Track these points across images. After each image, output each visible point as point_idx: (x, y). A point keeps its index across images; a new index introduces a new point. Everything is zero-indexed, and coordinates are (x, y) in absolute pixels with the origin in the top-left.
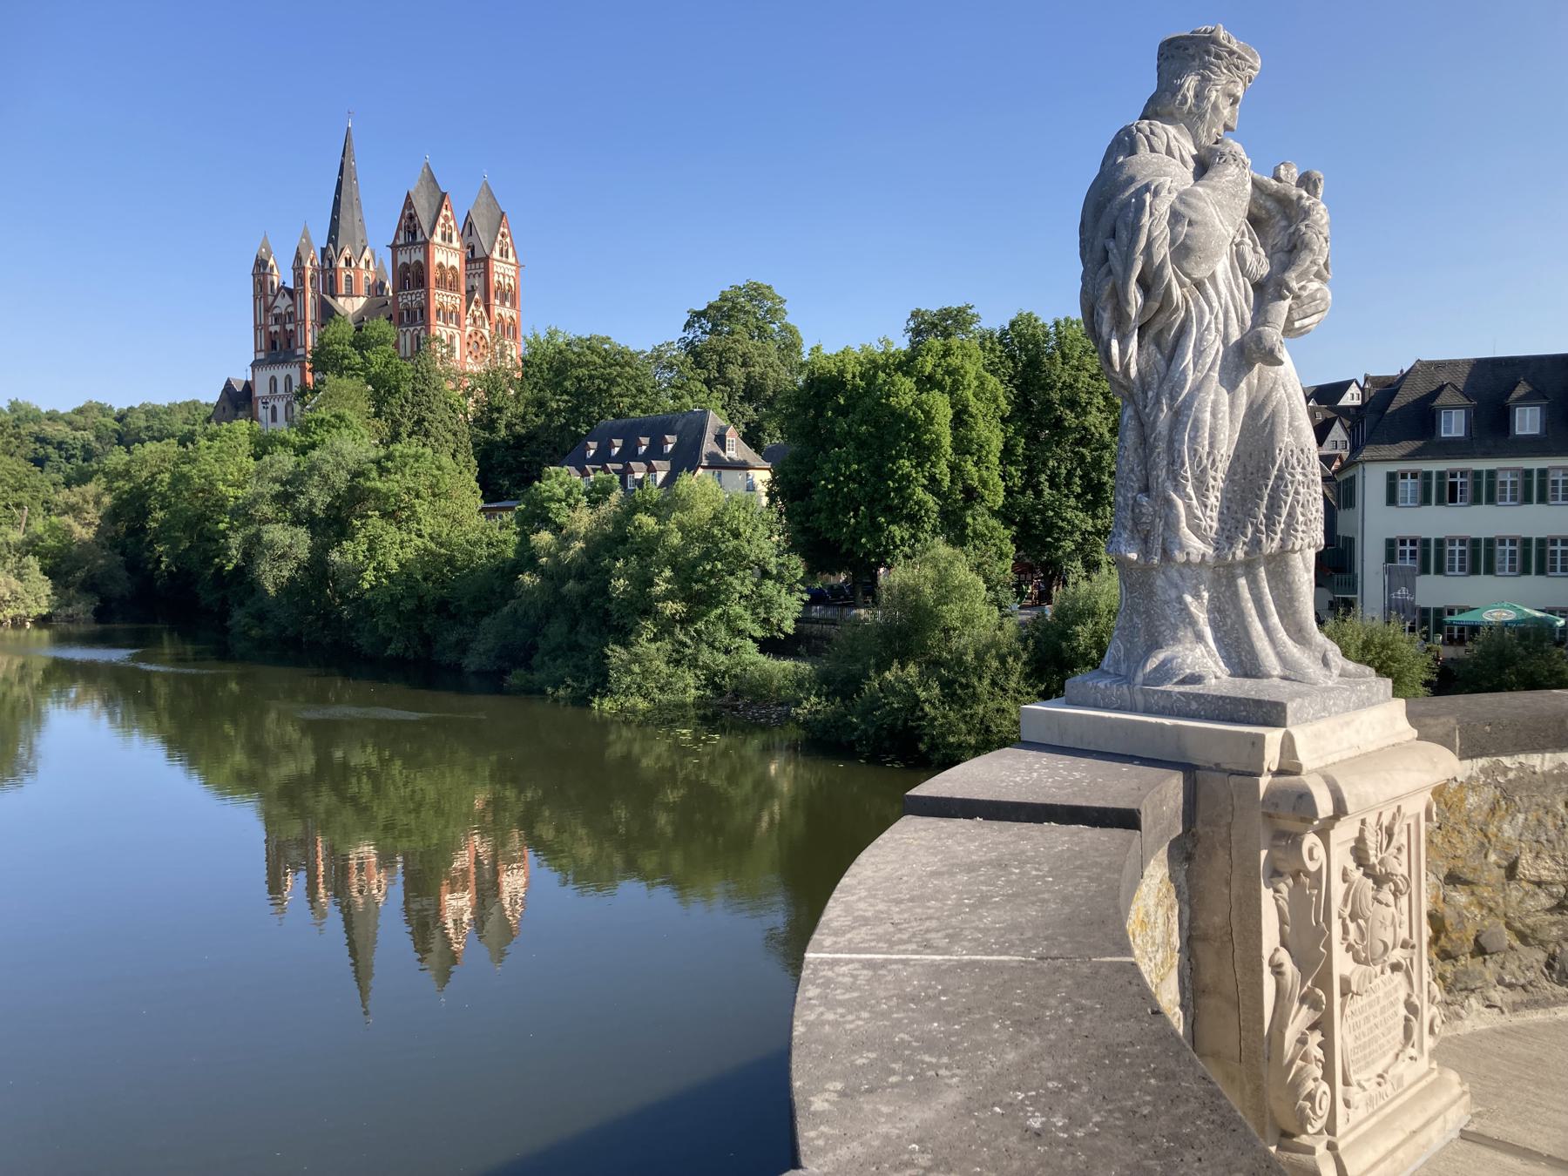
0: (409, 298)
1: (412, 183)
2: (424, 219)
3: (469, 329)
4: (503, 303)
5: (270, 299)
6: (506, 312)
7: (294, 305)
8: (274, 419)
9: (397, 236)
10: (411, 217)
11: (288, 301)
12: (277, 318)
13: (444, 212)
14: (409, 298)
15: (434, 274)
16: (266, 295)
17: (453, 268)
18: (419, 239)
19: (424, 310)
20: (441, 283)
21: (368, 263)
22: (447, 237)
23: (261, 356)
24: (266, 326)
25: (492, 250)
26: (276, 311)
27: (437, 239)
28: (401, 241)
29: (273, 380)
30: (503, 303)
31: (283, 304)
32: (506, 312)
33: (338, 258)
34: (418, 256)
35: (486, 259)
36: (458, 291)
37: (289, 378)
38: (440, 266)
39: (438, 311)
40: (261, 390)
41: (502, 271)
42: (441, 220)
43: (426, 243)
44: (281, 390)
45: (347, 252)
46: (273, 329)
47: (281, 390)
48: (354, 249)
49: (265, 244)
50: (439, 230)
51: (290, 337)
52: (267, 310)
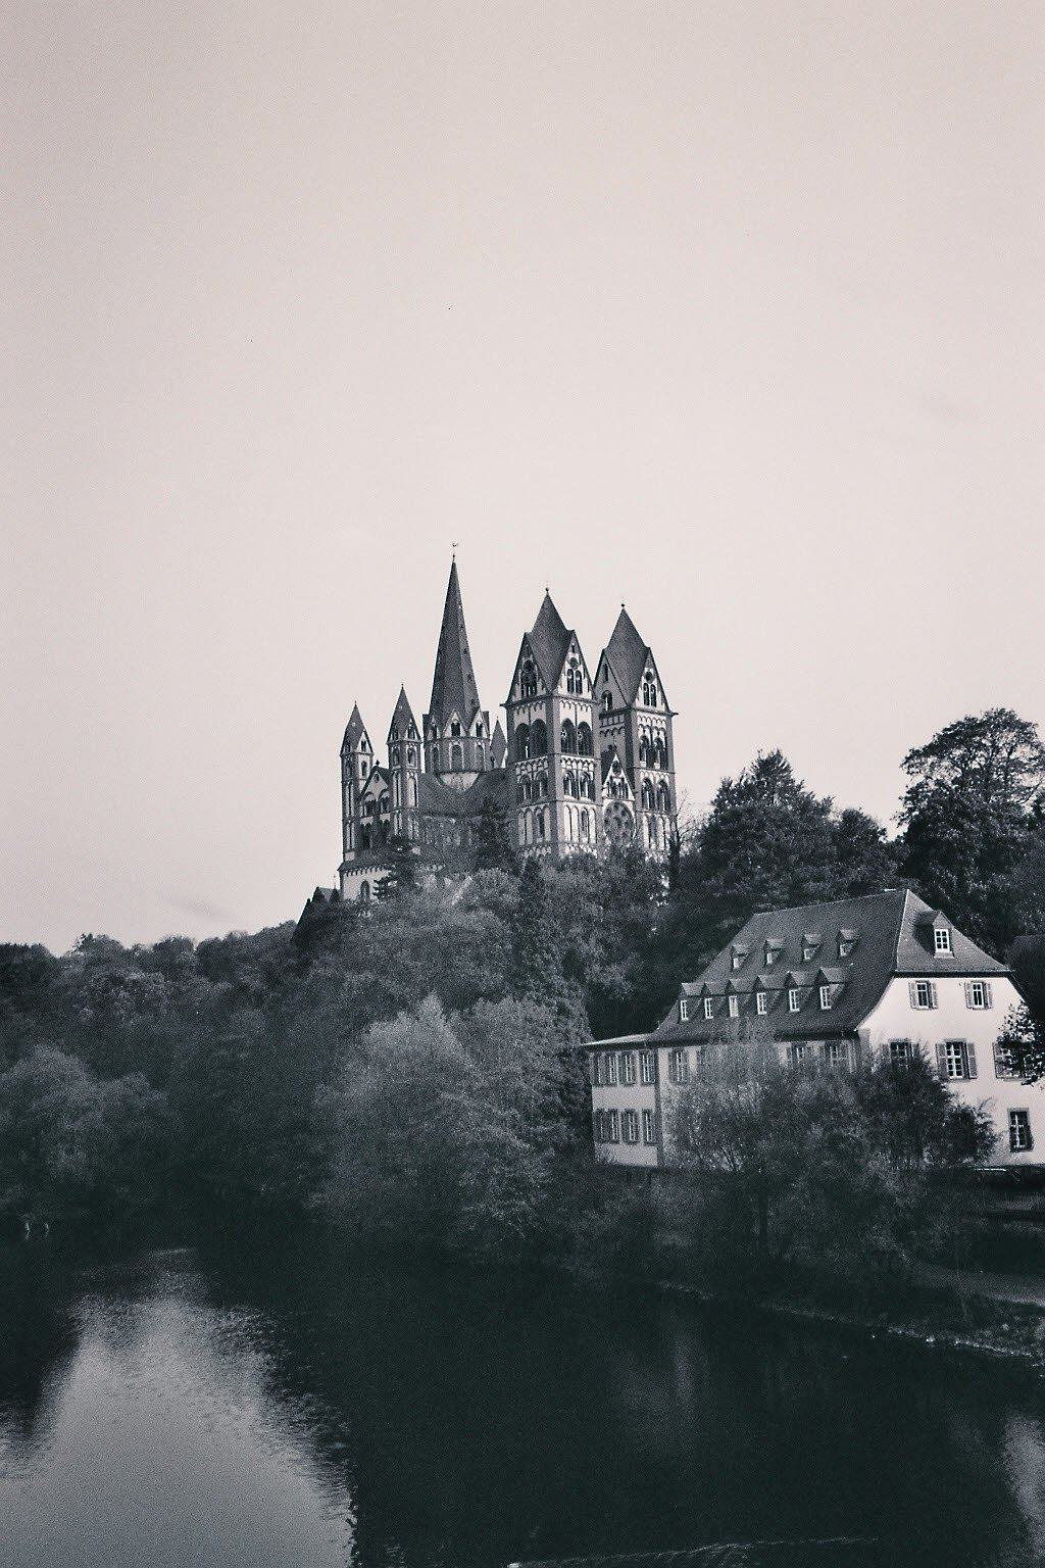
0: (529, 769)
2: (544, 665)
3: (607, 802)
4: (650, 765)
5: (362, 784)
6: (656, 776)
7: (390, 789)
9: (512, 692)
11: (382, 785)
12: (371, 806)
13: (570, 655)
15: (558, 736)
16: (356, 780)
17: (584, 725)
18: (541, 692)
19: (547, 782)
20: (567, 747)
21: (479, 729)
22: (575, 687)
23: (351, 856)
24: (358, 819)
25: (634, 696)
26: (369, 799)
27: (562, 690)
28: (518, 697)
29: (365, 884)
30: (650, 765)
31: (377, 788)
32: (656, 776)
33: (443, 726)
34: (539, 714)
35: (628, 711)
36: (591, 753)
38: (567, 723)
39: (565, 782)
41: (645, 722)
42: (567, 666)
43: (549, 697)
45: (455, 717)
46: (364, 822)
48: (462, 711)
49: (356, 716)
50: (564, 679)
52: (360, 797)
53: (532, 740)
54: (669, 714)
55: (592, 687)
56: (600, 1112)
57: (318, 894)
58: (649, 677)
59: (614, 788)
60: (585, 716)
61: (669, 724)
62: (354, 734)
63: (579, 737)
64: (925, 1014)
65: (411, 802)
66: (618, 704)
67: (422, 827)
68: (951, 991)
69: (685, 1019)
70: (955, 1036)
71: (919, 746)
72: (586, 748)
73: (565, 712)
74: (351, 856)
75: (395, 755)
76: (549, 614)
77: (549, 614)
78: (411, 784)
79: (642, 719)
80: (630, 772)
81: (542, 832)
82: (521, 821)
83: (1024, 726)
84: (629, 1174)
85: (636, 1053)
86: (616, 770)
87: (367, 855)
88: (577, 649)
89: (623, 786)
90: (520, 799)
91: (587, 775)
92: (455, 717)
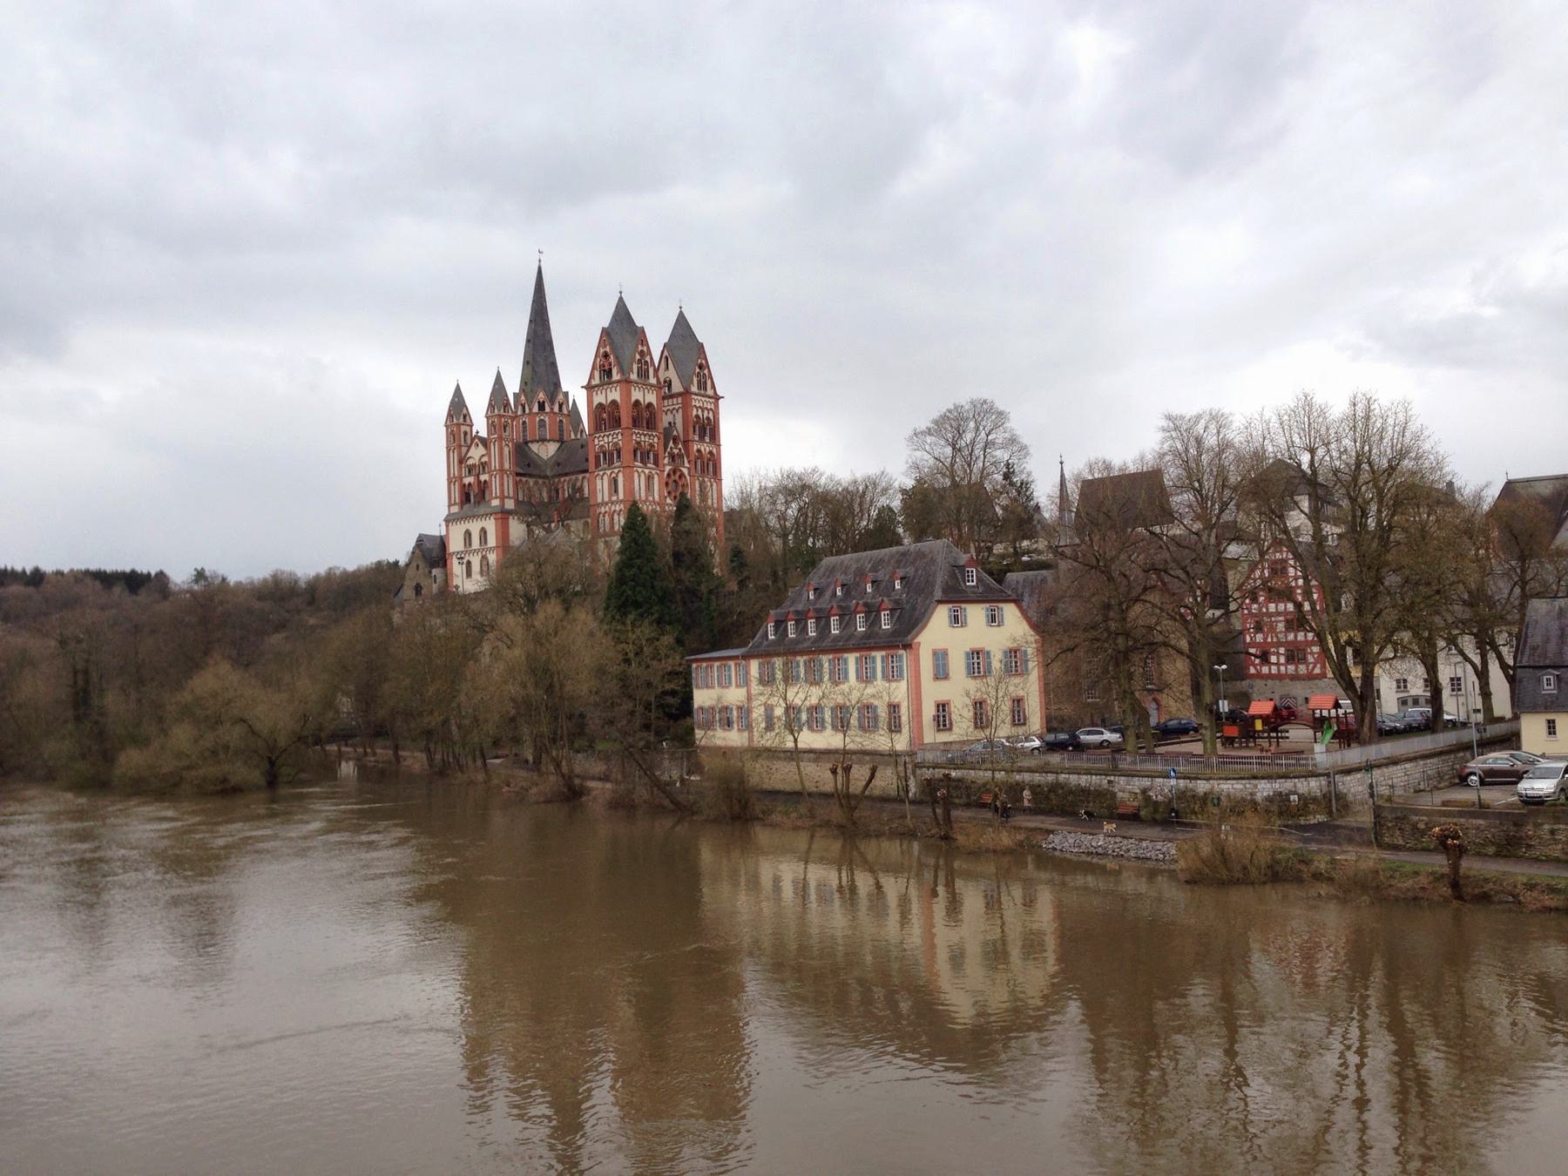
0: (605, 440)
1: (604, 317)
3: (668, 468)
4: (702, 438)
5: (464, 450)
6: (705, 448)
7: (489, 454)
8: (469, 574)
9: (592, 376)
10: (606, 355)
11: (481, 450)
12: (470, 469)
14: (605, 440)
17: (650, 405)
18: (616, 376)
20: (636, 422)
22: (643, 374)
23: (455, 509)
26: (470, 462)
28: (596, 381)
29: (468, 534)
30: (702, 438)
31: (476, 454)
32: (705, 448)
34: (615, 395)
35: (686, 393)
37: (484, 532)
38: (637, 403)
40: (456, 545)
44: (476, 543)
46: (467, 481)
47: (476, 543)
49: (458, 392)
51: (483, 488)
52: (460, 462)
53: (606, 417)
54: (717, 398)
55: (656, 371)
56: (702, 708)
57: (421, 540)
58: (701, 367)
59: (672, 457)
60: (651, 398)
61: (717, 406)
62: (458, 407)
63: (646, 415)
64: (959, 631)
65: (507, 466)
66: (677, 387)
67: (516, 484)
68: (976, 614)
69: (771, 637)
70: (977, 645)
71: (923, 428)
72: (651, 424)
73: (637, 395)
74: (455, 509)
75: (491, 426)
76: (622, 314)
77: (622, 314)
78: (506, 450)
79: (697, 401)
80: (686, 443)
81: (616, 491)
82: (599, 482)
83: (1000, 414)
84: (725, 752)
85: (732, 663)
86: (675, 440)
87: (466, 506)
88: (644, 341)
89: (681, 456)
90: (597, 464)
91: (652, 445)
92: (541, 396)
